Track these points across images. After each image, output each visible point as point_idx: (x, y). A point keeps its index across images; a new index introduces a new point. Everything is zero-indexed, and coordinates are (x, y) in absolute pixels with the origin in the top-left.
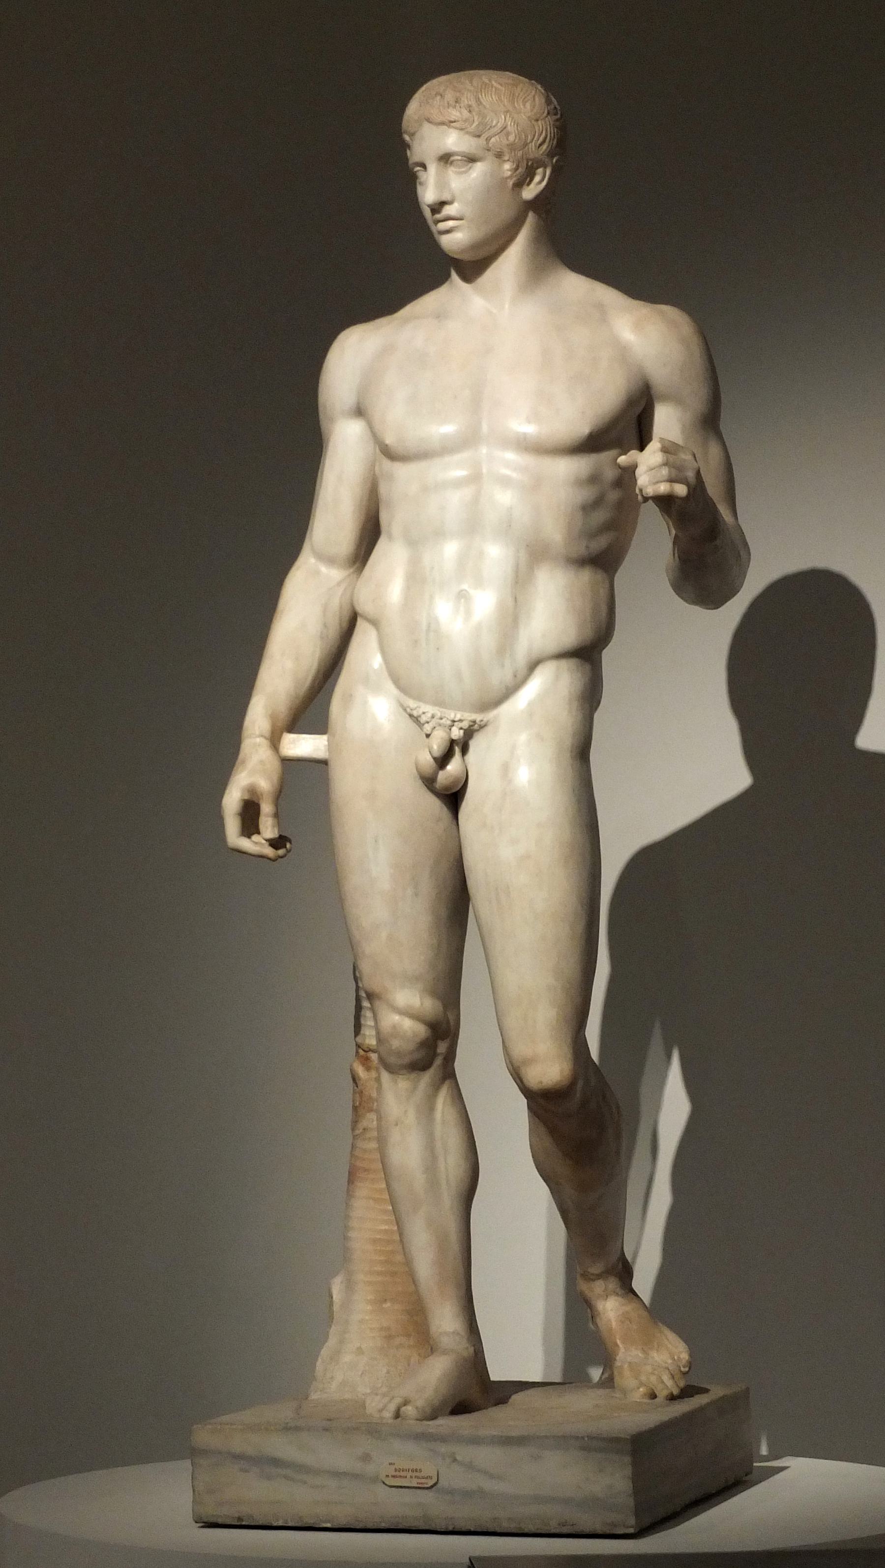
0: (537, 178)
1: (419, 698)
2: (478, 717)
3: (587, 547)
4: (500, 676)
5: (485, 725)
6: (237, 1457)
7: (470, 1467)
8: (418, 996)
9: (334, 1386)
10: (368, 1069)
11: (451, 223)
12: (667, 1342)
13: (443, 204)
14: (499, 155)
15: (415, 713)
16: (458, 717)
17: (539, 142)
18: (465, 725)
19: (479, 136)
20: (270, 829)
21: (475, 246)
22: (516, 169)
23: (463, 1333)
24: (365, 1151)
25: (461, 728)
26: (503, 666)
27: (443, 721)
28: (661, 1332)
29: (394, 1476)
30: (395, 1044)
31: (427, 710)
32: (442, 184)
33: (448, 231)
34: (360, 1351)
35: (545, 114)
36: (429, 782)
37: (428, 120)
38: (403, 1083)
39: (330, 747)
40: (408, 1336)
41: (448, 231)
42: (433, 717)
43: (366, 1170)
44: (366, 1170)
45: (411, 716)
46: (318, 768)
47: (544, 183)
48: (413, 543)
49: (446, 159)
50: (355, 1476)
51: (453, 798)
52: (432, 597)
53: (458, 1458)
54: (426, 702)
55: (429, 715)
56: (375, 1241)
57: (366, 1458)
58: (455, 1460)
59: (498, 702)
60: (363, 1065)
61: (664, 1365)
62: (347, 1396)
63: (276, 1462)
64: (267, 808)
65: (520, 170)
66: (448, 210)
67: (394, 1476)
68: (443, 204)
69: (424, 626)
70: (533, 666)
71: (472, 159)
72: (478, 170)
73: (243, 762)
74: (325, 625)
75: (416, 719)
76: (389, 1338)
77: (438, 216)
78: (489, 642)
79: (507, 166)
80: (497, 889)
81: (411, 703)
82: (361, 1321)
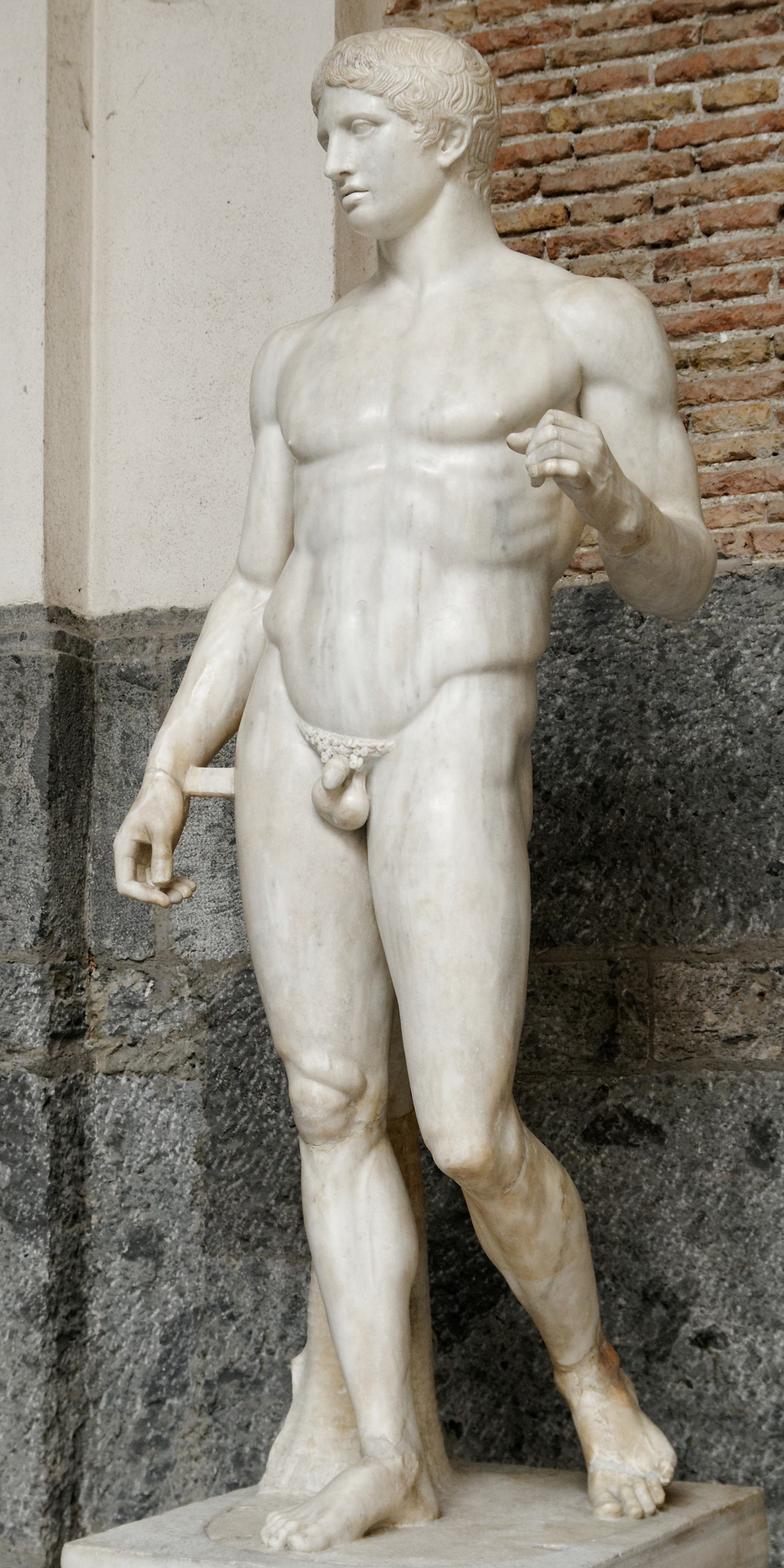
1: (316, 724)
2: (379, 743)
3: (504, 548)
5: (388, 752)
8: (327, 1058)
9: (284, 1481)
12: (649, 1447)
17: (453, 99)
18: (365, 751)
20: (159, 872)
22: (427, 130)
23: (390, 1440)
25: (360, 756)
26: (403, 683)
28: (645, 1434)
35: (462, 68)
36: (325, 818)
37: (329, 84)
39: (237, 781)
47: (463, 148)
48: (316, 553)
52: (328, 609)
55: (326, 742)
59: (401, 726)
61: (642, 1474)
62: (296, 1493)
64: (159, 849)
65: (431, 132)
69: (320, 641)
70: (439, 683)
74: (246, 650)
81: (310, 730)
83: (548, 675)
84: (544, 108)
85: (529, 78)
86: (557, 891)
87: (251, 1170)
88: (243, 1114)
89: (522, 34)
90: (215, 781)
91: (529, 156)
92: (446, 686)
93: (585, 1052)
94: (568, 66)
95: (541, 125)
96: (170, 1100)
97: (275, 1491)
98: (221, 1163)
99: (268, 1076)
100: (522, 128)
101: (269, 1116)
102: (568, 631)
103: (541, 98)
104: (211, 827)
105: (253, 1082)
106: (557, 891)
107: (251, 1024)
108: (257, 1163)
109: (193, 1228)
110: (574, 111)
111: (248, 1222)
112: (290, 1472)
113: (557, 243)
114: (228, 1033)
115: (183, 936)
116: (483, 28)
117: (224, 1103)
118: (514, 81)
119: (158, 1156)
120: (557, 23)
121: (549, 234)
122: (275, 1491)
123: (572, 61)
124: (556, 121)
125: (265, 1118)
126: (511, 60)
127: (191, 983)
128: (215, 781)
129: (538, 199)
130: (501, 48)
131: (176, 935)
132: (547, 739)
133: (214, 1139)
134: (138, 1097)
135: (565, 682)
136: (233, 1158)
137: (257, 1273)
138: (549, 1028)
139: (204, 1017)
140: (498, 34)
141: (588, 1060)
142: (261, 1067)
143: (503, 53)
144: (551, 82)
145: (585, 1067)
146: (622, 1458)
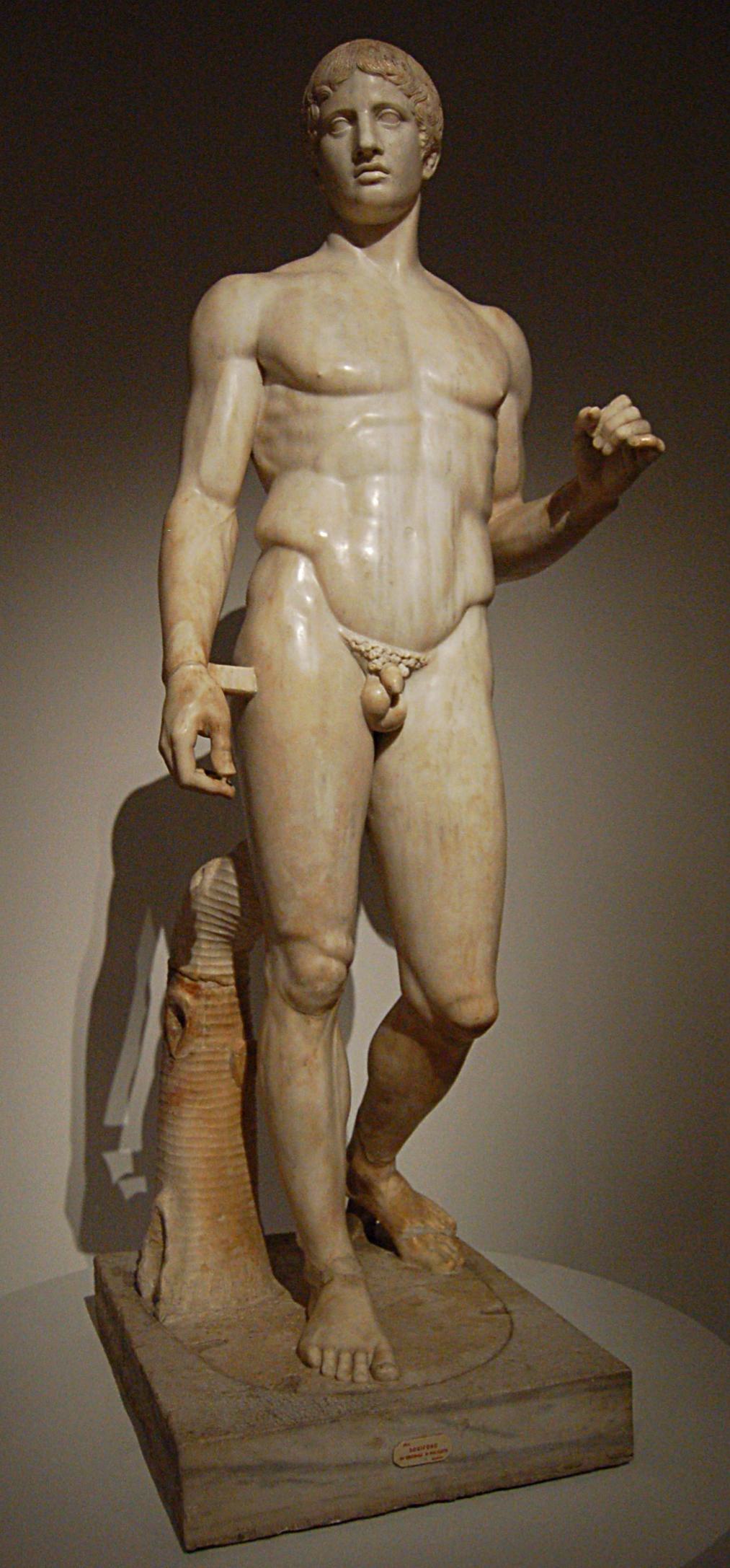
0: (430, 162)
4: (443, 617)
6: (234, 1470)
7: (484, 1430)
10: (197, 997)
11: (377, 174)
13: (376, 151)
14: (419, 123)
15: (363, 649)
16: (408, 654)
18: (411, 662)
19: (409, 97)
21: (394, 205)
24: (192, 1073)
26: (446, 606)
27: (393, 657)
29: (409, 1457)
30: (321, 986)
31: (373, 646)
32: (376, 135)
33: (373, 182)
34: (205, 1268)
37: (363, 70)
38: (315, 1024)
40: (243, 1245)
41: (373, 182)
42: (384, 651)
43: (193, 1092)
44: (193, 1092)
45: (353, 650)
46: (239, 702)
50: (366, 1464)
51: (383, 736)
53: (471, 1423)
54: (373, 637)
56: (208, 1159)
57: (378, 1442)
58: (468, 1427)
60: (191, 993)
63: (279, 1467)
66: (376, 160)
67: (409, 1457)
68: (376, 151)
70: (467, 607)
71: (402, 118)
72: (407, 128)
73: (189, 689)
75: (361, 656)
76: (229, 1250)
77: (366, 164)
78: (438, 580)
79: (422, 136)
80: (441, 828)
82: (201, 1239)
90: (239, 678)
92: (468, 613)
97: (180, 1318)
112: (189, 1298)
122: (180, 1318)
128: (239, 678)
146: (423, 1222)
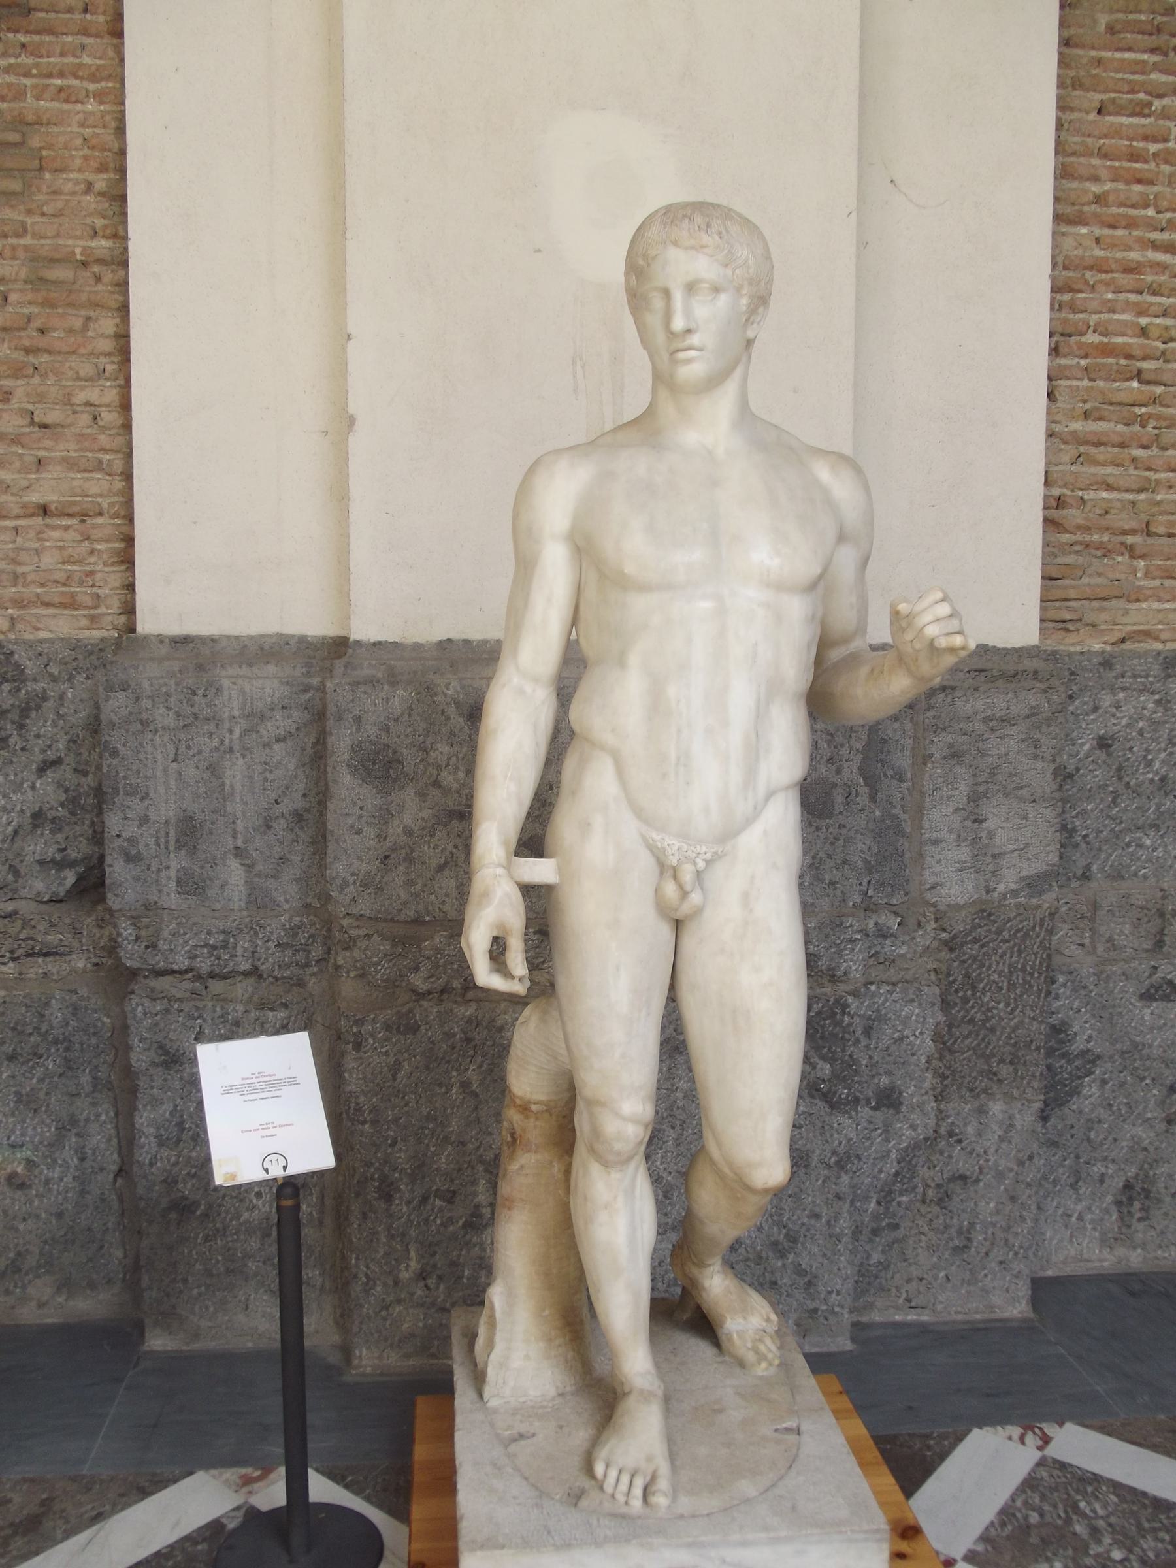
49: (691, 288)
83: (1135, 707)
84: (1144, 321)
85: (1133, 297)
86: (1128, 845)
87: (979, 1045)
88: (973, 1007)
89: (1133, 265)
91: (1137, 352)
93: (1145, 946)
94: (1162, 295)
95: (1144, 332)
96: (913, 1001)
98: (955, 1042)
99: (994, 981)
100: (1130, 332)
101: (993, 1008)
102: (1151, 679)
103: (1140, 314)
104: (957, 810)
105: (981, 986)
106: (1128, 845)
107: (982, 946)
108: (983, 1040)
109: (927, 1085)
110: (1167, 328)
111: (976, 1078)
113: (1150, 416)
114: (964, 954)
115: (933, 887)
116: (1101, 253)
117: (958, 1001)
118: (1122, 296)
119: (901, 1039)
120: (1158, 264)
121: (1143, 410)
123: (1166, 293)
124: (1155, 333)
125: (989, 1010)
126: (1125, 282)
127: (936, 920)
129: (1135, 384)
130: (1117, 272)
131: (928, 886)
132: (1131, 749)
133: (950, 1026)
134: (886, 1000)
135: (1145, 712)
136: (966, 1037)
137: (981, 1111)
138: (1121, 931)
139: (946, 943)
140: (1116, 261)
141: (1147, 951)
142: (989, 976)
143: (1116, 275)
144: (1151, 304)
145: (1144, 955)
